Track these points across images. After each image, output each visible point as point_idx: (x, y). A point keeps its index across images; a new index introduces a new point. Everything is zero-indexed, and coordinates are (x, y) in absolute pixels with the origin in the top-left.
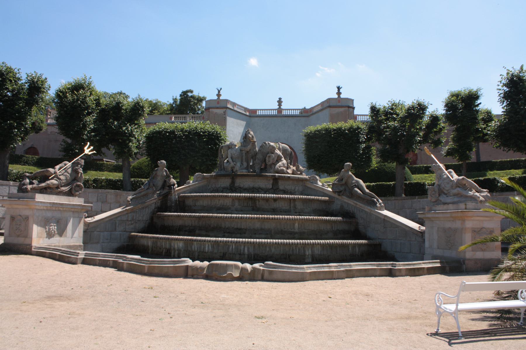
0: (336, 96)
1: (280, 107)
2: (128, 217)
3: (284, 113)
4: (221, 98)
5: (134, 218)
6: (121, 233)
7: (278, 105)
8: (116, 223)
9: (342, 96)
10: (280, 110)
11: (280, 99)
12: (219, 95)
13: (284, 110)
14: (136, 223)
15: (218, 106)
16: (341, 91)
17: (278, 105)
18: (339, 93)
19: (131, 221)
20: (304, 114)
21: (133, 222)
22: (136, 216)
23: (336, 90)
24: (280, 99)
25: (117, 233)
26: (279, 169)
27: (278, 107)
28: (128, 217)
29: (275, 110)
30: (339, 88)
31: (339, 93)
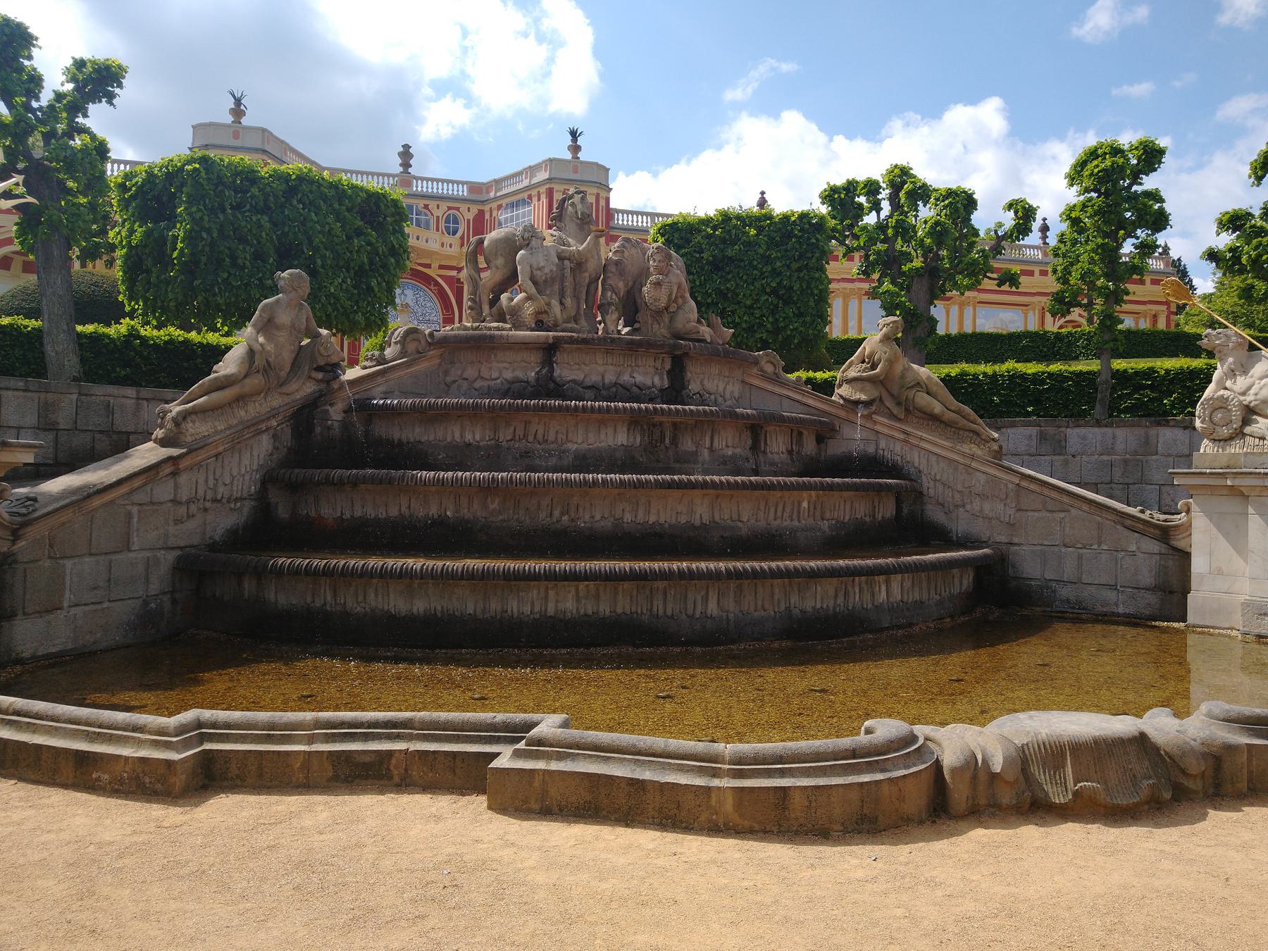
0: (568, 156)
1: (406, 172)
2: (176, 487)
3: (419, 187)
4: (245, 121)
5: (201, 492)
6: (148, 554)
7: (401, 165)
8: (129, 515)
9: (583, 156)
10: (406, 177)
11: (406, 147)
12: (238, 111)
13: (417, 178)
14: (206, 510)
15: (237, 143)
16: (580, 141)
17: (401, 165)
18: (575, 148)
19: (188, 502)
20: (474, 197)
21: (193, 508)
22: (206, 481)
23: (568, 139)
24: (406, 147)
25: (131, 555)
26: (687, 326)
27: (401, 169)
28: (176, 487)
29: (394, 176)
30: (574, 134)
31: (575, 148)
